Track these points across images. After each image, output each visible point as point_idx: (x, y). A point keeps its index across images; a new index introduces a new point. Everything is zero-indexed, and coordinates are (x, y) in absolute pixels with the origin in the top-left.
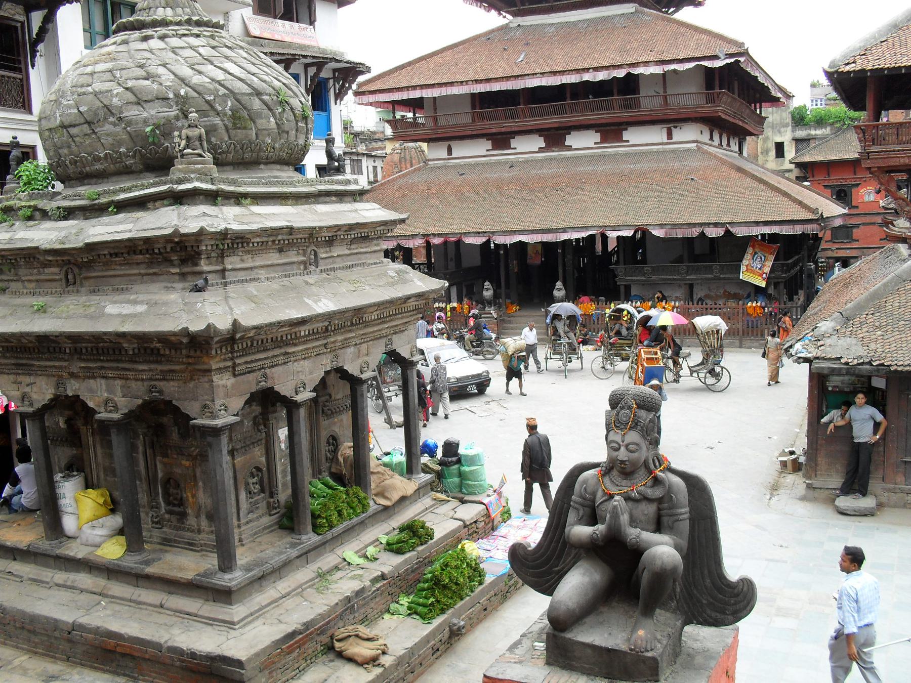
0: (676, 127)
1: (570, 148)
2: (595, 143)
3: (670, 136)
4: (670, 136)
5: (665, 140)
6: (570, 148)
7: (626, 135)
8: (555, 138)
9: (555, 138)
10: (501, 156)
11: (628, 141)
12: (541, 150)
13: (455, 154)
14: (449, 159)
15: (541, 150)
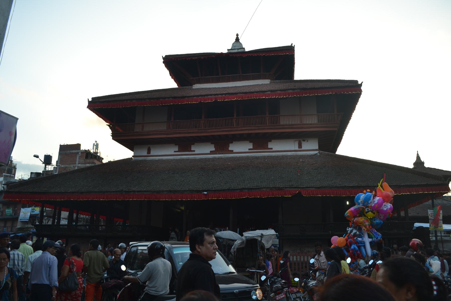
0: (304, 141)
1: (232, 152)
2: (249, 149)
3: (300, 146)
4: (300, 146)
5: (297, 148)
6: (232, 152)
7: (270, 145)
8: (222, 143)
9: (222, 143)
10: (185, 156)
11: (272, 149)
12: (212, 153)
13: (152, 153)
14: (147, 156)
15: (212, 153)
